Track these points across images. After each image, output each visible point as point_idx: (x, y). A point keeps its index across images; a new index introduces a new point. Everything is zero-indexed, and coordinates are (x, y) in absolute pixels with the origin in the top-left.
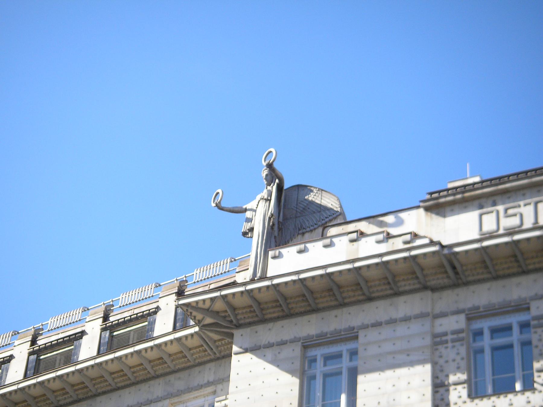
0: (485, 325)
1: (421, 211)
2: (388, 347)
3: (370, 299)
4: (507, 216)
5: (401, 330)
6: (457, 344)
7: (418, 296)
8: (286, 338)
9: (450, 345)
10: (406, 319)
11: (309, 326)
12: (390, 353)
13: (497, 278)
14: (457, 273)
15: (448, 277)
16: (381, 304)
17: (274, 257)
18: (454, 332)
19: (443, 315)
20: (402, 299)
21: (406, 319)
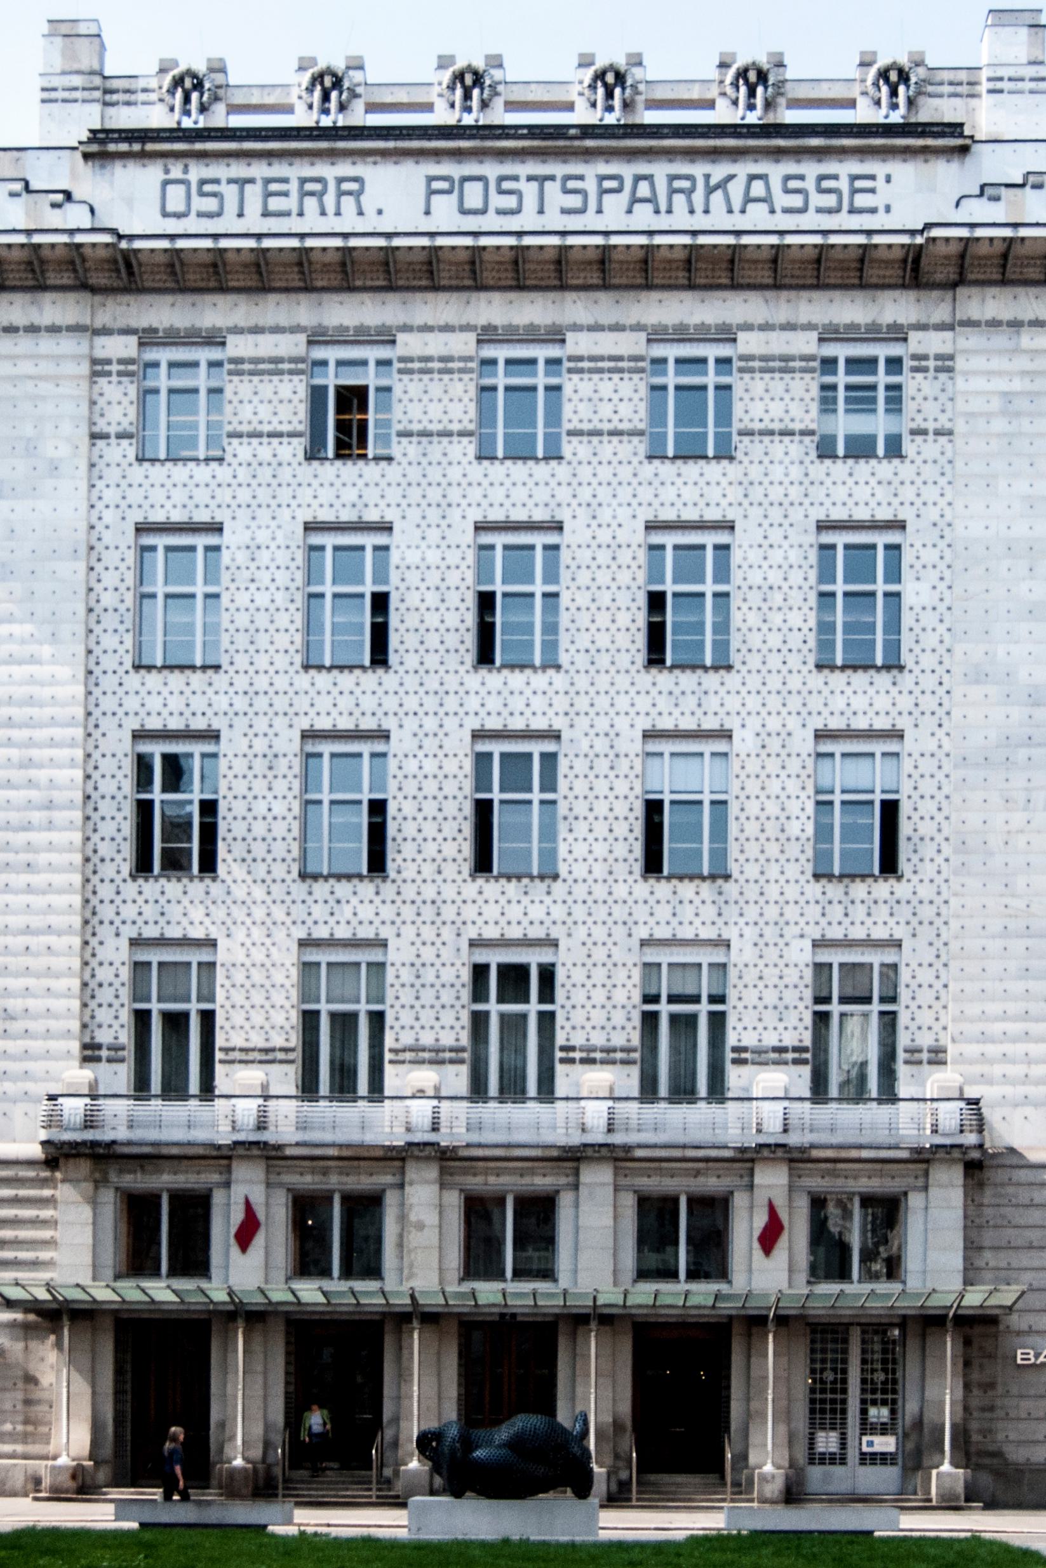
0: (164, 355)
1: (78, 155)
2: (26, 367)
4: (202, 194)
5: (47, 344)
6: (125, 379)
7: (72, 297)
9: (114, 378)
10: (54, 329)
12: (31, 377)
14: (131, 273)
15: (119, 277)
16: (19, 298)
18: (121, 362)
19: (105, 331)
20: (48, 297)
21: (54, 329)
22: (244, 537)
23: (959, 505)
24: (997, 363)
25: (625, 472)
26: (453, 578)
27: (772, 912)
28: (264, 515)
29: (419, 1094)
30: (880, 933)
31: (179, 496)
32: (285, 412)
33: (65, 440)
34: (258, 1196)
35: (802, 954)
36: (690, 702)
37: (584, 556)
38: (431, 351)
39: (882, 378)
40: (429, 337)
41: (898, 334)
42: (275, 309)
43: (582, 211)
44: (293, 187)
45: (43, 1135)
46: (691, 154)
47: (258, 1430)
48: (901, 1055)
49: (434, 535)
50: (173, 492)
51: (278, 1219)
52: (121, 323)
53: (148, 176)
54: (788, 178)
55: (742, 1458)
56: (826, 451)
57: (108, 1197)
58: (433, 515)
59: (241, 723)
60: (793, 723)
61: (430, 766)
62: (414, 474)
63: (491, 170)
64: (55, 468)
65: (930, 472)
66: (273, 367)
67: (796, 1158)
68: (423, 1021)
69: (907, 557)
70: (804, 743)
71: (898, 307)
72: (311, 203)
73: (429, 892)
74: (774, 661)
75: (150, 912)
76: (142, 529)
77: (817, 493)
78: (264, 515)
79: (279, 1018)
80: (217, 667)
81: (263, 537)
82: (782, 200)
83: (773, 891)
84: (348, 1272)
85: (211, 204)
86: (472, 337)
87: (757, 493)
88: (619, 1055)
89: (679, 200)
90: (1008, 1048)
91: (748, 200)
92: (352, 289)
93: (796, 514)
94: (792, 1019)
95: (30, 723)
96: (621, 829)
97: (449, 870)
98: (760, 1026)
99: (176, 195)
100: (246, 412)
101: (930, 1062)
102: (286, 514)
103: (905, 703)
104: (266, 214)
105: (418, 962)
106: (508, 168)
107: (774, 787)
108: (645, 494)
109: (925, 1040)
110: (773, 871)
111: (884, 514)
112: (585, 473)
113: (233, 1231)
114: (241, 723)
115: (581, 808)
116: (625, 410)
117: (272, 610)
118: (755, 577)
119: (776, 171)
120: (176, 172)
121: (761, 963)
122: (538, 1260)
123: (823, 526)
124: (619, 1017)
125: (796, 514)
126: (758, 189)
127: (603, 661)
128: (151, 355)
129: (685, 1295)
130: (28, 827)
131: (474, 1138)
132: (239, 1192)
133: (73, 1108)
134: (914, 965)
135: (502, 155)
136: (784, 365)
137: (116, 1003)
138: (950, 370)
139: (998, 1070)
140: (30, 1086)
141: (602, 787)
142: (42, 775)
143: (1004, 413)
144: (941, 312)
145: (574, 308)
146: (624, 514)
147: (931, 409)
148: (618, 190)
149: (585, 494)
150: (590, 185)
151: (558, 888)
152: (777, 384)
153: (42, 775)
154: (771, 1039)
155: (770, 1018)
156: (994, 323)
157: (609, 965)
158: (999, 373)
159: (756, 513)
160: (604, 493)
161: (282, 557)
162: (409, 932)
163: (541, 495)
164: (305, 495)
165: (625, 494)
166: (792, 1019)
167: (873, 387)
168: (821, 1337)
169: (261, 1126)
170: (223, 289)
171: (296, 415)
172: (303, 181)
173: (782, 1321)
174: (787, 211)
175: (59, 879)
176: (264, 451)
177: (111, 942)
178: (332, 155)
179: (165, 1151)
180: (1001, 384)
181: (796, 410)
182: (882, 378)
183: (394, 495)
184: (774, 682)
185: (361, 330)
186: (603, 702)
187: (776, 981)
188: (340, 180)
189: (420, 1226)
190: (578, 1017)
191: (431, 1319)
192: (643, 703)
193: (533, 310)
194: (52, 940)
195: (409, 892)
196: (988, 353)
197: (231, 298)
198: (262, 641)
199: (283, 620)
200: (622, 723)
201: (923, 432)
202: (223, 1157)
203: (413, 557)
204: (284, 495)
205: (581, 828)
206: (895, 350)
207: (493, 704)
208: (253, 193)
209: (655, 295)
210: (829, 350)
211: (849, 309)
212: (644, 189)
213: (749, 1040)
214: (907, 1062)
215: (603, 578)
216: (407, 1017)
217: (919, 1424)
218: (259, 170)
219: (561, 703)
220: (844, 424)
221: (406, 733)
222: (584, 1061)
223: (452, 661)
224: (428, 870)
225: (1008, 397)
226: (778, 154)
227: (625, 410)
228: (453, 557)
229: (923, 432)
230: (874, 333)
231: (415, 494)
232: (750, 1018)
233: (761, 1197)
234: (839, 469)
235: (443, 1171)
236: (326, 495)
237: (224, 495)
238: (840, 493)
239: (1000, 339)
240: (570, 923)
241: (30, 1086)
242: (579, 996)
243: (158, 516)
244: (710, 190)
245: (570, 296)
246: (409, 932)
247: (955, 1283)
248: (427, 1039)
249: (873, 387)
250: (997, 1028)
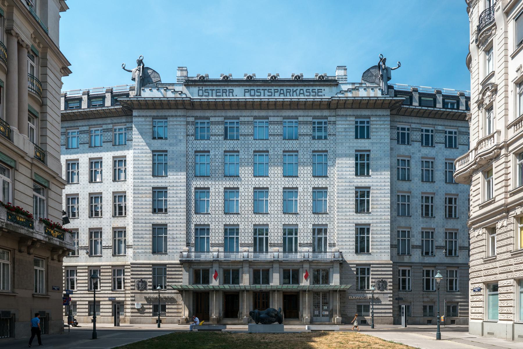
0: (199, 121)
2: (175, 123)
3: (170, 109)
5: (179, 119)
7: (183, 110)
8: (148, 115)
10: (180, 116)
11: (154, 113)
13: (202, 109)
17: (143, 90)
19: (189, 117)
20: (179, 110)
21: (180, 116)
22: (213, 153)
23: (337, 148)
24: (343, 123)
25: (279, 142)
26: (250, 161)
27: (305, 220)
28: (217, 149)
29: (245, 251)
30: (324, 223)
31: (202, 146)
32: (220, 131)
33: (182, 136)
34: (217, 269)
35: (310, 227)
36: (291, 183)
37: (272, 157)
38: (245, 120)
39: (323, 125)
40: (245, 118)
41: (326, 117)
42: (218, 113)
43: (271, 95)
44: (221, 91)
45: (180, 259)
46: (290, 86)
48: (328, 245)
49: (246, 153)
50: (201, 145)
51: (221, 274)
52: (192, 115)
53: (195, 89)
54: (307, 90)
55: (302, 315)
56: (314, 138)
57: (191, 270)
58: (246, 149)
59: (214, 186)
60: (309, 186)
61: (246, 194)
62: (243, 142)
63: (256, 88)
64: (180, 141)
65: (332, 142)
66: (218, 123)
69: (328, 157)
70: (311, 190)
71: (326, 113)
72: (224, 94)
73: (246, 216)
74: (305, 175)
75: (198, 220)
76: (196, 152)
77: (312, 146)
78: (217, 149)
80: (209, 176)
81: (217, 153)
82: (306, 94)
83: (306, 216)
84: (233, 283)
85: (207, 94)
86: (252, 118)
87: (302, 146)
89: (288, 94)
90: (346, 243)
91: (300, 94)
92: (232, 109)
93: (309, 149)
94: (309, 238)
95: (177, 186)
96: (279, 205)
97: (250, 212)
99: (201, 92)
100: (214, 131)
102: (221, 149)
103: (328, 183)
104: (216, 96)
106: (258, 88)
107: (306, 197)
108: (283, 146)
110: (306, 212)
111: (324, 149)
112: (272, 142)
114: (214, 186)
115: (272, 201)
116: (279, 131)
117: (219, 166)
118: (302, 160)
119: (305, 89)
120: (201, 88)
122: (267, 280)
123: (314, 151)
124: (279, 238)
125: (309, 149)
126: (302, 92)
127: (276, 175)
128: (197, 121)
129: (292, 287)
130: (177, 204)
131: (255, 259)
132: (214, 269)
133: (185, 254)
135: (257, 86)
136: (306, 123)
138: (335, 124)
139: (345, 247)
140: (178, 250)
141: (276, 197)
142: (179, 195)
143: (344, 131)
144: (334, 114)
145: (270, 113)
146: (279, 149)
147: (332, 131)
148: (277, 92)
149: (272, 146)
150: (273, 91)
151: (269, 216)
152: (305, 127)
153: (179, 195)
154: (306, 242)
155: (305, 238)
156: (343, 115)
158: (344, 124)
159: (302, 149)
160: (276, 146)
161: (220, 157)
162: (243, 223)
163: (265, 146)
164: (224, 146)
165: (279, 146)
167: (322, 127)
168: (315, 294)
169: (218, 257)
170: (209, 109)
171: (222, 132)
172: (223, 90)
173: (309, 291)
174: (307, 96)
175: (182, 214)
176: (217, 138)
178: (228, 86)
180: (344, 126)
181: (309, 131)
182: (323, 125)
183: (239, 146)
184: (305, 179)
185: (233, 116)
186: (276, 183)
188: (229, 90)
190: (272, 238)
191: (248, 291)
192: (283, 183)
193: (263, 113)
194: (181, 224)
195: (243, 216)
196: (342, 121)
197: (211, 111)
198: (217, 171)
199: (220, 168)
200: (279, 186)
201: (331, 135)
203: (243, 157)
204: (220, 146)
205: (272, 205)
206: (326, 120)
207: (257, 183)
208: (214, 92)
209: (284, 111)
210: (314, 120)
211: (318, 113)
212: (282, 92)
213: (302, 242)
215: (276, 161)
216: (243, 238)
217: (332, 310)
218: (215, 88)
219: (269, 183)
220: (317, 134)
221: (242, 188)
223: (250, 176)
224: (246, 212)
225: (345, 128)
226: (305, 86)
227: (279, 131)
228: (250, 157)
229: (331, 135)
230: (322, 117)
231: (243, 146)
232: (302, 238)
233: (305, 269)
234: (316, 141)
235: (249, 265)
236: (228, 146)
237: (210, 146)
238: (316, 146)
239: (344, 119)
240: (271, 222)
241: (178, 250)
242: (272, 234)
243: (199, 149)
244: (293, 92)
245: (269, 111)
246: (243, 223)
247: (338, 284)
248: (246, 242)
249: (322, 127)
250: (344, 239)
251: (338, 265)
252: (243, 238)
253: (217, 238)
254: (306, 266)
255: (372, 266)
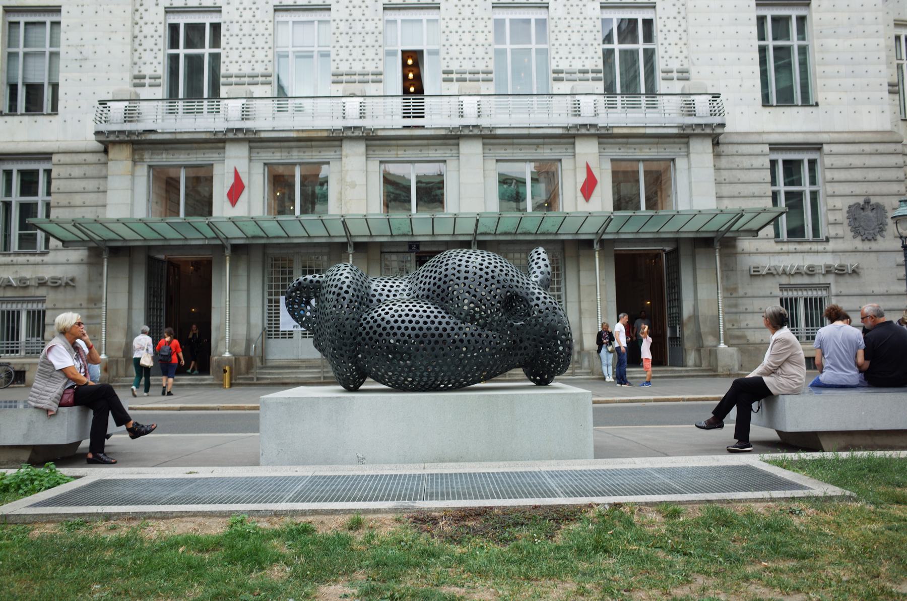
34: (243, 167)
47: (242, 331)
57: (142, 171)
67: (605, 136)
68: (354, 56)
79: (260, 55)
88: (481, 76)
94: (590, 52)
98: (570, 56)
101: (678, 79)
105: (350, 19)
109: (675, 65)
113: (227, 190)
121: (569, 17)
124: (480, 52)
134: (664, 18)
137: (156, 48)
154: (577, 65)
155: (576, 52)
157: (473, 19)
166: (590, 52)
177: (153, 10)
179: (179, 137)
187: (579, 28)
189: (353, 185)
202: (217, 142)
213: (564, 65)
214: (664, 79)
222: (458, 80)
232: (563, 52)
248: (357, 67)
251: (708, 145)
252: (344, 54)
253: (247, 55)
254: (587, 150)
255: (826, 148)
